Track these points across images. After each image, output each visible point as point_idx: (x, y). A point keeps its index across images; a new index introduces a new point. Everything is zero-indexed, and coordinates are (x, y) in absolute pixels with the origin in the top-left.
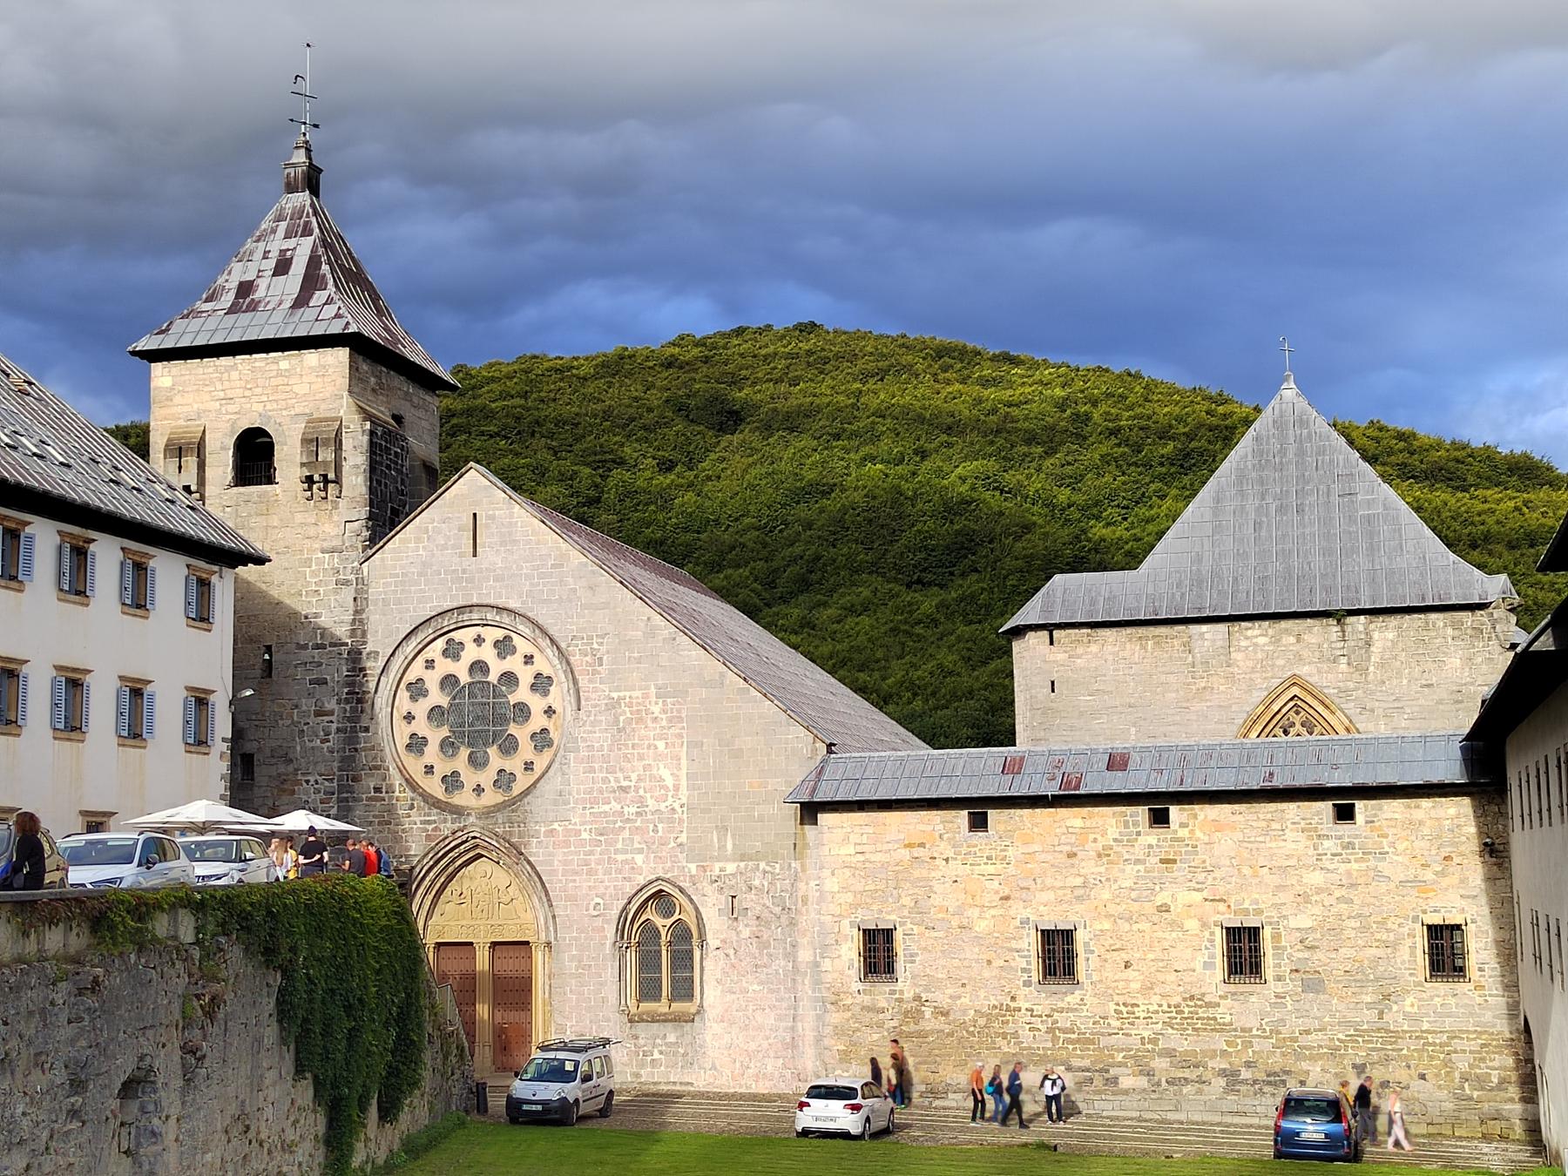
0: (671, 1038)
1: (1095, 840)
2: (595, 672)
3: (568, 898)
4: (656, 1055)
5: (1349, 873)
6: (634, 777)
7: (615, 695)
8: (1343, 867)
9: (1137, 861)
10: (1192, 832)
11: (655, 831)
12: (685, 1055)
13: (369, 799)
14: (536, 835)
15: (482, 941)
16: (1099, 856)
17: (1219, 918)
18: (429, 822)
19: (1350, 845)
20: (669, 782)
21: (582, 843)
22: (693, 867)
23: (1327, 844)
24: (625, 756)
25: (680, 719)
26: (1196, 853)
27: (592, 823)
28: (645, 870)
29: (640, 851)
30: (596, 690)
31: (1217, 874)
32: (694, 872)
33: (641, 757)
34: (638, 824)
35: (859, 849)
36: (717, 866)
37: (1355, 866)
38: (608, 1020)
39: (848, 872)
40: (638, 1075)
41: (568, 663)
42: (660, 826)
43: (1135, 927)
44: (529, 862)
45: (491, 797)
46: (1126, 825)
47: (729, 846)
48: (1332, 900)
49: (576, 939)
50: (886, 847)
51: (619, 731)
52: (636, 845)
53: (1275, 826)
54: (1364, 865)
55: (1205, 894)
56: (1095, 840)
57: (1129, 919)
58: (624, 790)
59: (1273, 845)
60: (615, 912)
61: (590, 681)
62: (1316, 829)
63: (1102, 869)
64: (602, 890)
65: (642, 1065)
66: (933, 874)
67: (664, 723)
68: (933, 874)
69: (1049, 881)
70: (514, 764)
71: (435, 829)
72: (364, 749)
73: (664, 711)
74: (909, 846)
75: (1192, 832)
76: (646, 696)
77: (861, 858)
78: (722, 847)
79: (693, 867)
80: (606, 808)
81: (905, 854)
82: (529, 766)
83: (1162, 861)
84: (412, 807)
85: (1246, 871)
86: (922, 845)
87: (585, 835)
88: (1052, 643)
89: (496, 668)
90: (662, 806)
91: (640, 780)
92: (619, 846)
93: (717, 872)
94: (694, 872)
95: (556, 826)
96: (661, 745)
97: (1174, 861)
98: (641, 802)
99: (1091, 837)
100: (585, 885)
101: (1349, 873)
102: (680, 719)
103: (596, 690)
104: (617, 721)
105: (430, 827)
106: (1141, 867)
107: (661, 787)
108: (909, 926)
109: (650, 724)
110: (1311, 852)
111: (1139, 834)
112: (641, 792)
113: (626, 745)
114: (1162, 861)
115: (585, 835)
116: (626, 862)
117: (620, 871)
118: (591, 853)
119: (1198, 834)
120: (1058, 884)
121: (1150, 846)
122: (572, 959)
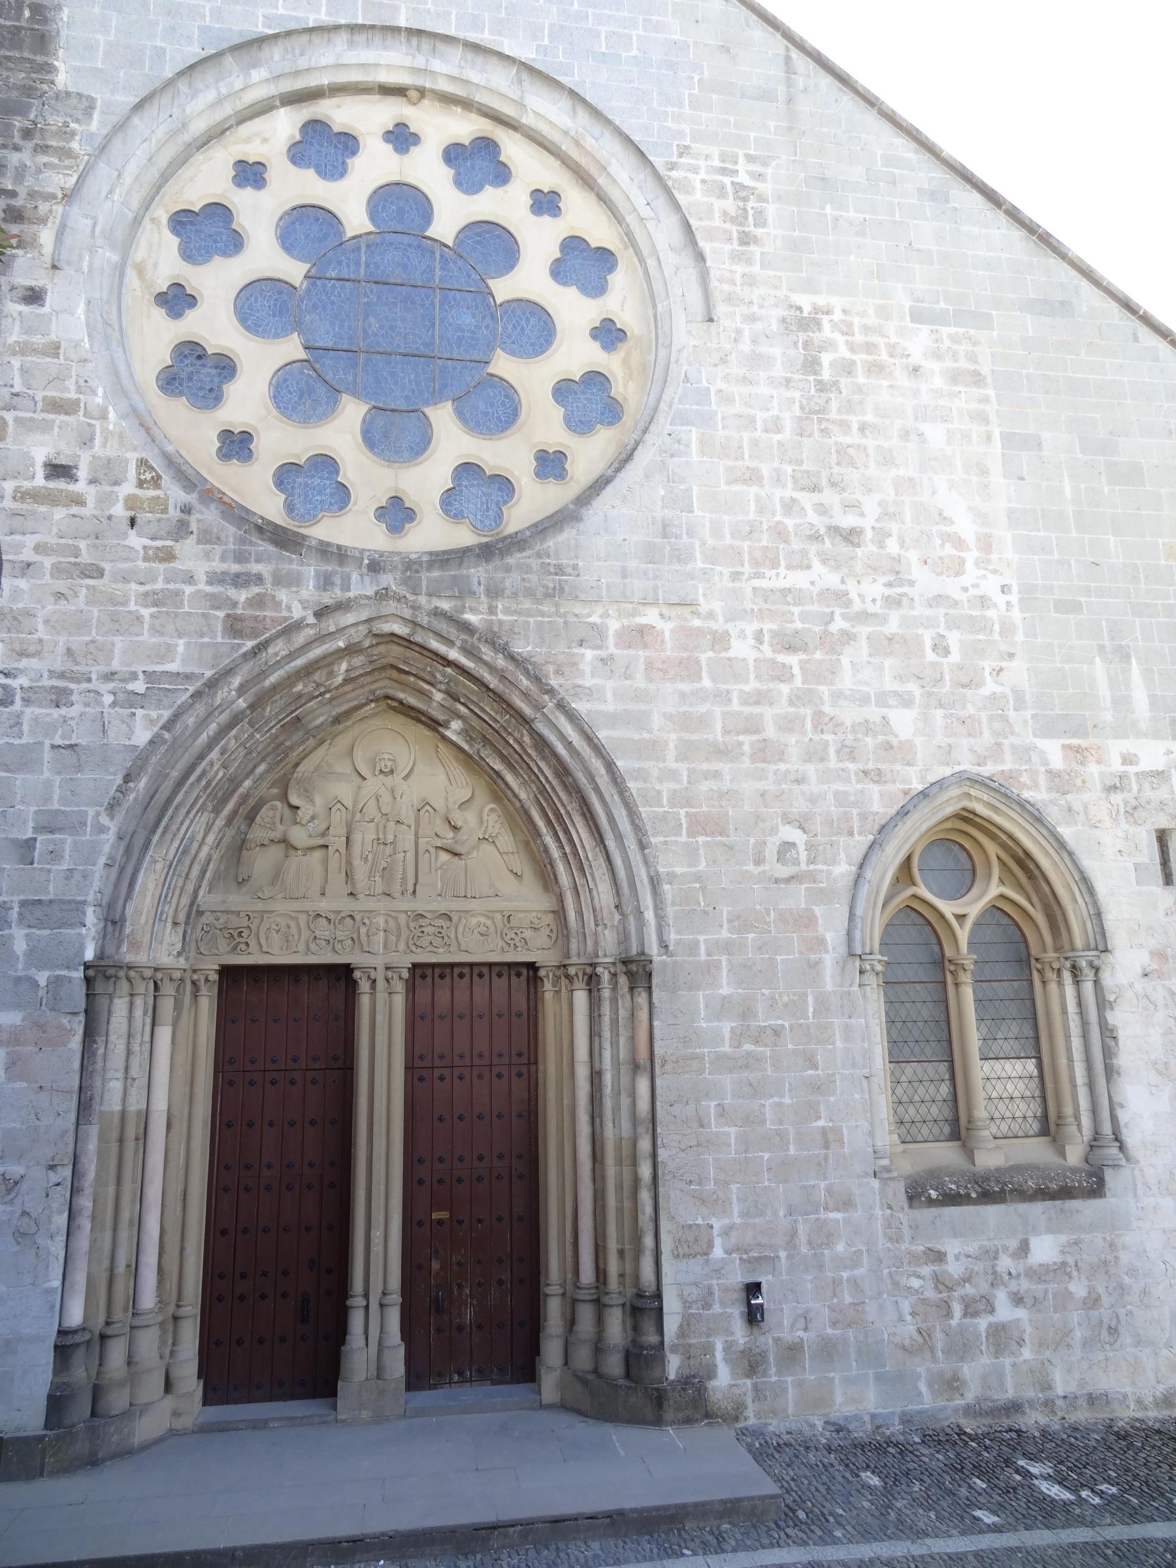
0: (1045, 1249)
2: (746, 239)
3: (698, 825)
4: (1005, 1311)
6: (871, 506)
7: (805, 301)
11: (941, 648)
12: (1092, 1301)
13: (22, 495)
14: (593, 636)
15: (383, 958)
18: (240, 581)
20: (966, 527)
21: (732, 670)
22: (1053, 752)
24: (841, 450)
25: (977, 379)
27: (761, 615)
28: (930, 751)
29: (906, 701)
30: (750, 281)
32: (1057, 760)
33: (887, 459)
34: (893, 626)
36: (1115, 748)
38: (847, 1204)
40: (952, 1384)
41: (677, 207)
42: (954, 639)
44: (572, 716)
45: (432, 533)
47: (1140, 698)
49: (727, 947)
51: (822, 387)
52: (890, 685)
58: (851, 536)
60: (843, 869)
61: (736, 257)
64: (800, 806)
65: (961, 1347)
67: (938, 382)
70: (510, 455)
71: (259, 602)
72: (24, 349)
73: (938, 356)
76: (884, 312)
78: (1121, 702)
79: (1053, 752)
80: (798, 580)
82: (550, 464)
84: (181, 530)
87: (741, 649)
89: (452, 211)
90: (952, 587)
91: (886, 515)
92: (846, 681)
93: (1116, 766)
94: (1057, 760)
95: (650, 617)
96: (935, 433)
98: (896, 573)
100: (749, 787)
102: (977, 379)
103: (750, 281)
104: (812, 365)
105: (242, 596)
107: (947, 538)
109: (902, 379)
112: (892, 546)
113: (845, 426)
115: (741, 649)
116: (867, 728)
117: (849, 752)
118: (761, 698)
122: (723, 1007)
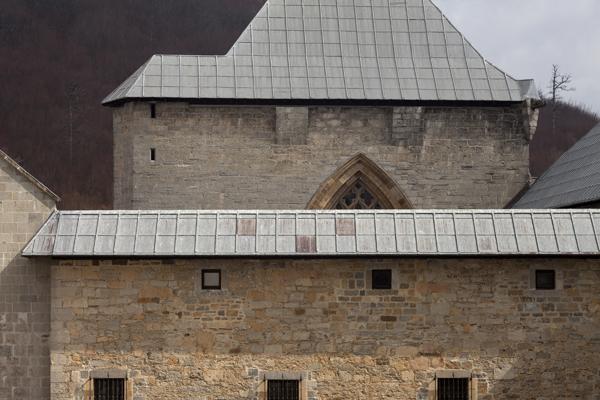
1: (322, 299)
5: (547, 331)
8: (543, 327)
9: (361, 319)
10: (411, 292)
16: (326, 312)
17: (430, 370)
19: (550, 307)
23: (530, 305)
26: (414, 312)
31: (433, 331)
35: (93, 302)
37: (553, 326)
39: (80, 325)
43: (358, 378)
46: (352, 285)
48: (532, 355)
50: (119, 301)
53: (485, 288)
54: (561, 325)
55: (421, 349)
56: (322, 299)
57: (350, 371)
59: (483, 305)
62: (520, 292)
63: (328, 325)
66: (166, 328)
68: (166, 328)
69: (278, 335)
74: (143, 300)
75: (411, 292)
77: (95, 311)
81: (138, 308)
83: (383, 319)
85: (458, 328)
86: (156, 300)
88: (153, 116)
97: (394, 319)
99: (319, 295)
101: (547, 331)
106: (364, 324)
108: (140, 376)
110: (516, 312)
111: (362, 293)
114: (383, 319)
119: (418, 295)
120: (287, 338)
121: (373, 305)
